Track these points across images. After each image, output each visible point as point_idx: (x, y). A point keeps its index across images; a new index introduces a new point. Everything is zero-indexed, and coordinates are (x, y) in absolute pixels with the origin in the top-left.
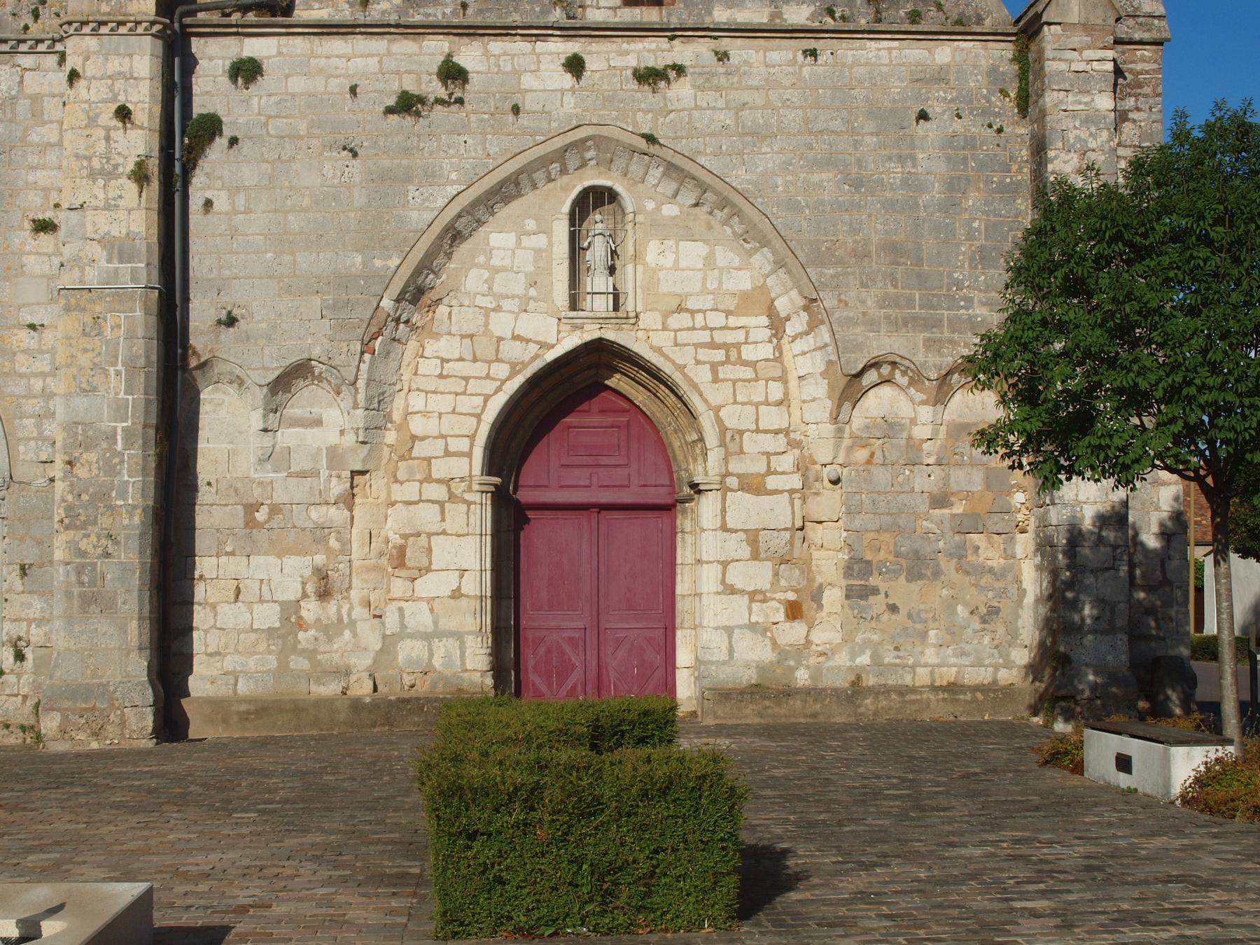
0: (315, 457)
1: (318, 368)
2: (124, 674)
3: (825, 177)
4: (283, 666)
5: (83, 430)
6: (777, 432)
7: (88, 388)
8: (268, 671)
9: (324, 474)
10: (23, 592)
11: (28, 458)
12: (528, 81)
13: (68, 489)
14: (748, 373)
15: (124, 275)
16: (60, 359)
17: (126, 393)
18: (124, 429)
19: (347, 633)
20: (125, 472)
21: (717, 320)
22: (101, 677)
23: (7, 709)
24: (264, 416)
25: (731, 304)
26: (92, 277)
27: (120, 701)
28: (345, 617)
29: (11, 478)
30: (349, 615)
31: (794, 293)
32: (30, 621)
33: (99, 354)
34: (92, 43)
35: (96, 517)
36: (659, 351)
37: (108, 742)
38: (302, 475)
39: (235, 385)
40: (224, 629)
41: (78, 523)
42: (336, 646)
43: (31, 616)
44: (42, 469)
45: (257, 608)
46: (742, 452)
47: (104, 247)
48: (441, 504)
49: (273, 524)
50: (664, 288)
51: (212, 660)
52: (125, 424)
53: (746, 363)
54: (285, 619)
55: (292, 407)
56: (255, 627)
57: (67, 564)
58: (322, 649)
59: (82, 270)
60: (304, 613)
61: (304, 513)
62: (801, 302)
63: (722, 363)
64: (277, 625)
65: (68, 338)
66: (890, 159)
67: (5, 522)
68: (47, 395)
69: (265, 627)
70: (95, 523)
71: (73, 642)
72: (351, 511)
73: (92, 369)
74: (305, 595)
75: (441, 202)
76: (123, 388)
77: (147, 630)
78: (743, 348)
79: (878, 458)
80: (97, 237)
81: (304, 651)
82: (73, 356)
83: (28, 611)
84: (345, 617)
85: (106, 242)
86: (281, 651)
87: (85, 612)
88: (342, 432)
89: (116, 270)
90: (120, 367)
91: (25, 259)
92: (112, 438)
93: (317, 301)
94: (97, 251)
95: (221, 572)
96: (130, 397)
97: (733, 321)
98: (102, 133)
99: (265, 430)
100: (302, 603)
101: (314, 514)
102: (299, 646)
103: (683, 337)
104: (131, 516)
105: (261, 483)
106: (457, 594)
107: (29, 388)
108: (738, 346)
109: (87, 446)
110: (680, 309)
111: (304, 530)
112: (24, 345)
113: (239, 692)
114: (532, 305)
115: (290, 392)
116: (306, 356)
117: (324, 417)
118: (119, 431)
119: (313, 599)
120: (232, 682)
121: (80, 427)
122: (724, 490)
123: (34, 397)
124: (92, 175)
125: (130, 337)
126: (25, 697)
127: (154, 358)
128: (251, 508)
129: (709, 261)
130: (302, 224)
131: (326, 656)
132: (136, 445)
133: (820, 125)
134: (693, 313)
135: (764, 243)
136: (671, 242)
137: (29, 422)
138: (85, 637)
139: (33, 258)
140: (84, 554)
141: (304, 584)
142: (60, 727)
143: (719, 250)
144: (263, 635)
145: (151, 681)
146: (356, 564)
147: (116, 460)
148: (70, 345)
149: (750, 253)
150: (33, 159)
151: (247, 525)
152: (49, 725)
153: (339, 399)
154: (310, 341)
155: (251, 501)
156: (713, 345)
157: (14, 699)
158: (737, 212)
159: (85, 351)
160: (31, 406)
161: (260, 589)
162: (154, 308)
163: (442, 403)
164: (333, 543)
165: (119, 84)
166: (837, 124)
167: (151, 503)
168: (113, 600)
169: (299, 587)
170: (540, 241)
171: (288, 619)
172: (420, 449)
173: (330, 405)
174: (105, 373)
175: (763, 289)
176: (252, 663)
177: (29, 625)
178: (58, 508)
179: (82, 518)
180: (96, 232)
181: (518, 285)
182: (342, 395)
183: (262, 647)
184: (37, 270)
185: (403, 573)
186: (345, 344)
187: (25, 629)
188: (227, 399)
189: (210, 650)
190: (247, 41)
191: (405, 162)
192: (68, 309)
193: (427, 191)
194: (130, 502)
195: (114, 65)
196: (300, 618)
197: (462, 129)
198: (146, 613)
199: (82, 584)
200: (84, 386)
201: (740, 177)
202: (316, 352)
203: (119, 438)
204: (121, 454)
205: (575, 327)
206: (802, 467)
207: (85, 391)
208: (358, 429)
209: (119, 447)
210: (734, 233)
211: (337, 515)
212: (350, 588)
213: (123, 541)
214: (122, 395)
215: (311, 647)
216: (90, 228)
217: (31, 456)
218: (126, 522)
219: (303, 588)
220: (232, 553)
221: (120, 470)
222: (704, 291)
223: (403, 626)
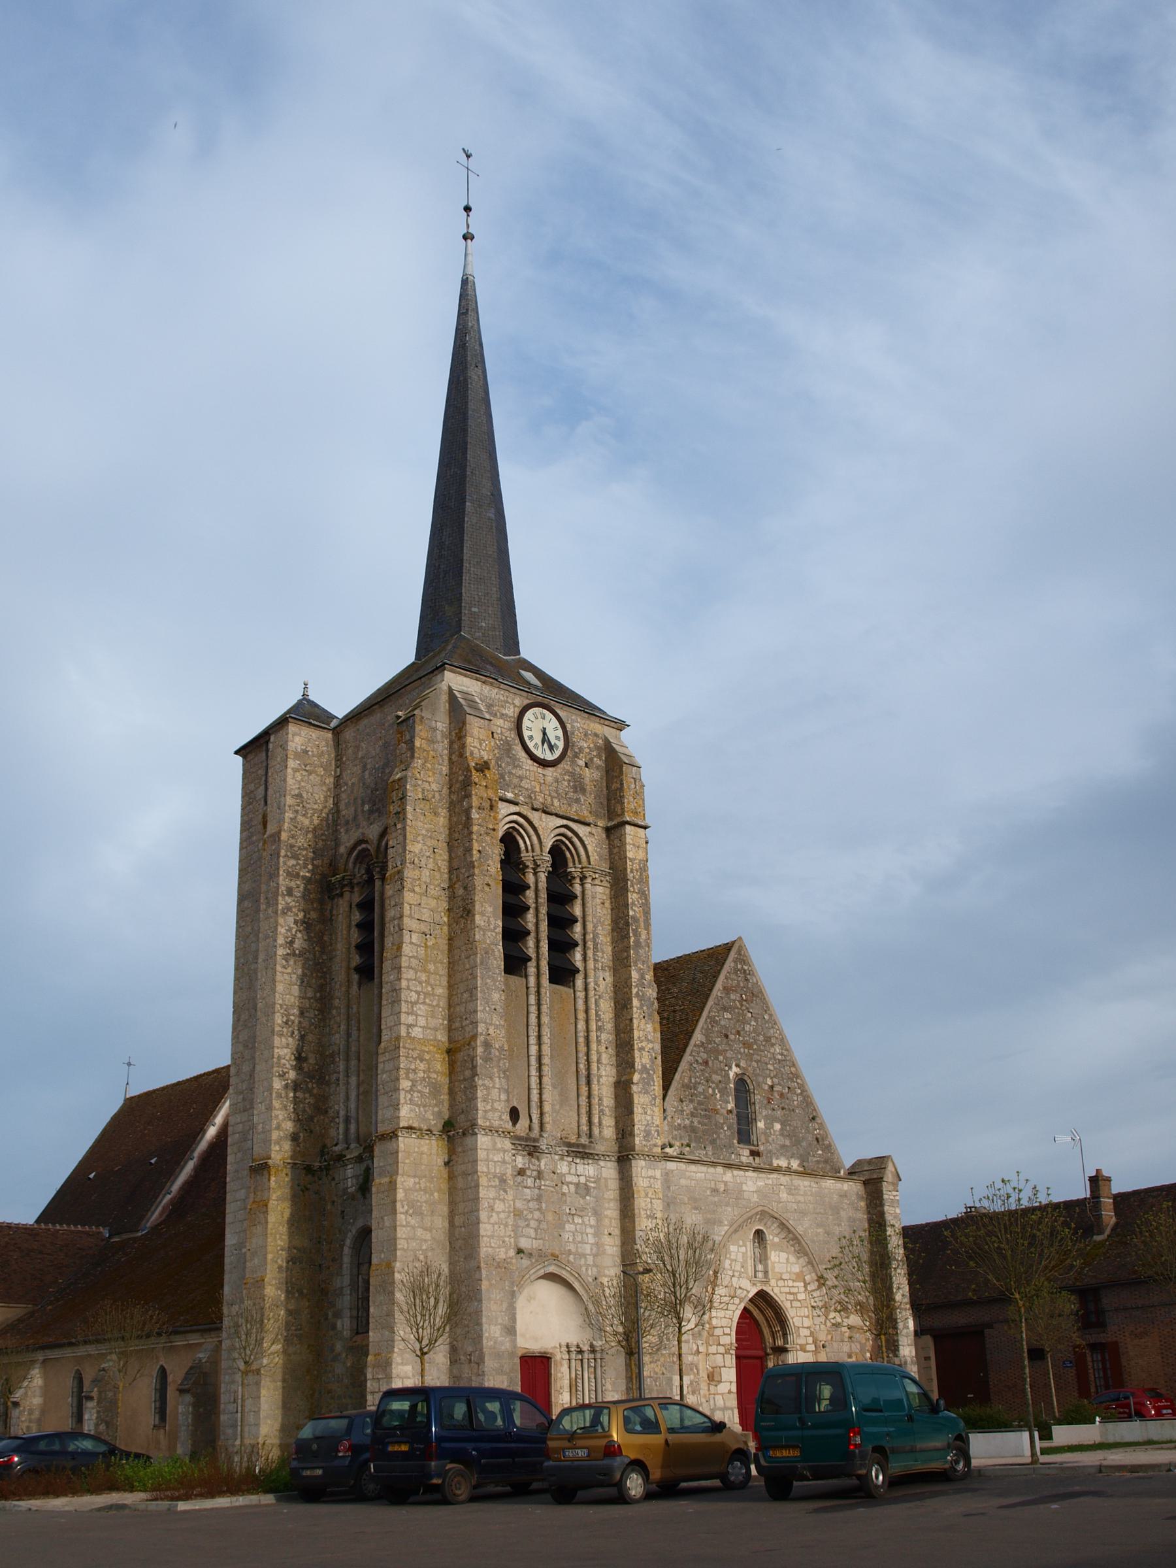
3: (820, 1230)
6: (807, 1328)
9: (691, 1341)
12: (745, 1187)
14: (799, 1304)
21: (791, 1283)
25: (794, 1277)
31: (814, 1275)
34: (642, 1163)
36: (776, 1294)
46: (799, 1336)
48: (723, 1354)
50: (777, 1270)
53: (799, 1301)
62: (816, 1278)
63: (793, 1300)
66: (835, 1225)
70: (659, 1360)
75: (723, 1233)
78: (798, 1295)
79: (834, 1339)
97: (796, 1284)
98: (649, 1200)
103: (783, 1290)
106: (730, 1392)
108: (796, 1293)
110: (781, 1279)
114: (743, 1275)
122: (796, 1351)
124: (648, 1217)
129: (788, 1259)
133: (818, 1211)
134: (784, 1280)
135: (806, 1254)
136: (777, 1253)
139: (608, 1247)
140: (657, 1374)
143: (790, 1256)
149: (798, 1258)
150: (607, 1205)
156: (790, 1293)
158: (799, 1243)
163: (721, 1314)
165: (652, 1180)
166: (822, 1211)
170: (743, 1249)
172: (718, 1332)
175: (802, 1272)
181: (738, 1268)
185: (714, 1383)
190: (668, 1163)
191: (713, 1216)
193: (720, 1228)
195: (651, 1172)
197: (727, 1205)
201: (800, 1229)
205: (754, 1284)
206: (815, 1342)
210: (795, 1250)
222: (787, 1272)
223: (715, 1405)
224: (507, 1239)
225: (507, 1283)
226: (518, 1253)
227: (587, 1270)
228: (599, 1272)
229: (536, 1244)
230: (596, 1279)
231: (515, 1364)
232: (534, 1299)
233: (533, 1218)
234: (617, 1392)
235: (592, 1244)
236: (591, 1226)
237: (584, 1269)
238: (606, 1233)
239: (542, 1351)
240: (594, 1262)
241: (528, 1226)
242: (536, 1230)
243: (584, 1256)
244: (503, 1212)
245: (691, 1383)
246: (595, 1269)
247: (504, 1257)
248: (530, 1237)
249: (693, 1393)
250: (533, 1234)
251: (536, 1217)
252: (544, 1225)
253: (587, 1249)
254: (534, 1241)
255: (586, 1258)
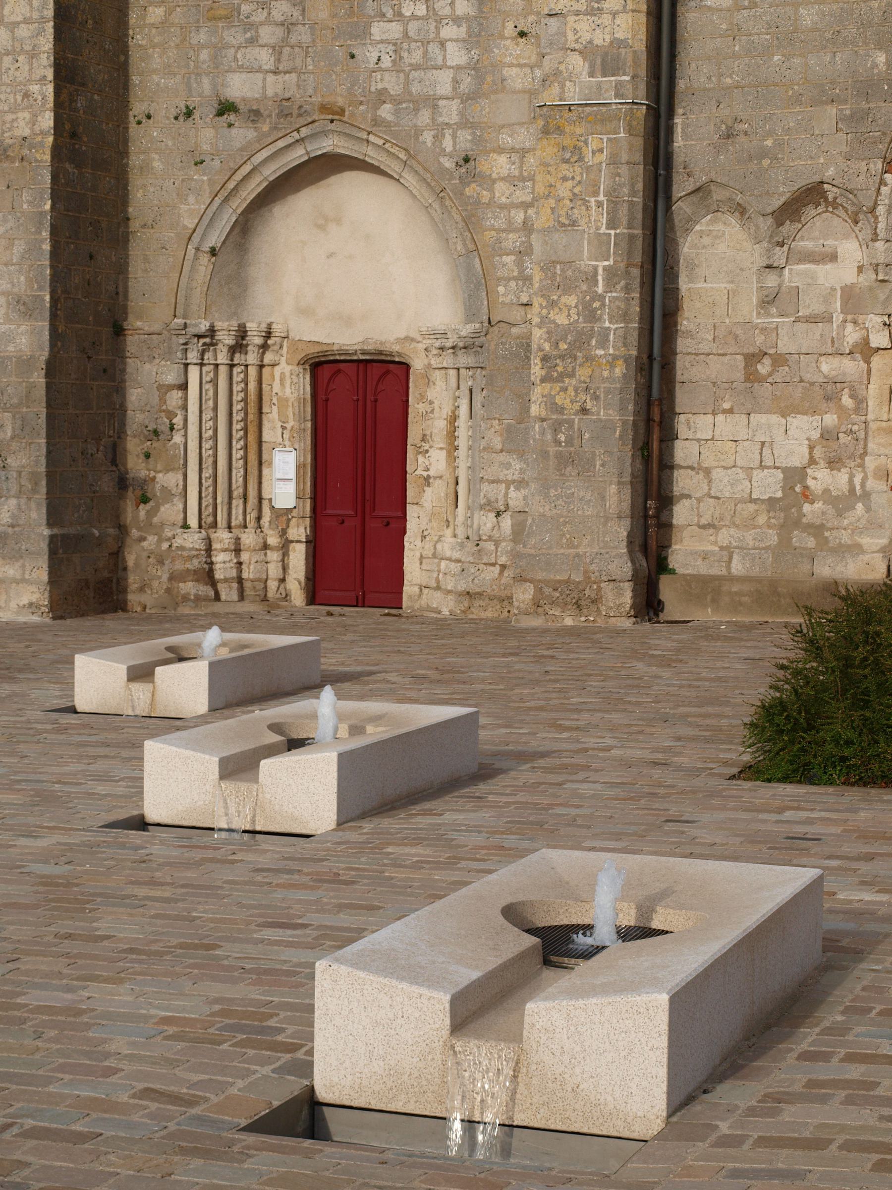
0: (827, 299)
1: (832, 193)
2: (602, 545)
4: (785, 541)
5: (562, 270)
7: (567, 222)
8: (766, 548)
9: (838, 318)
10: (502, 451)
11: (507, 300)
13: (545, 336)
15: (607, 90)
16: (540, 189)
17: (607, 228)
18: (605, 269)
19: (860, 506)
20: (606, 317)
22: (577, 547)
23: (484, 579)
24: (768, 250)
26: (573, 96)
27: (597, 574)
28: (858, 487)
29: (490, 323)
30: (863, 485)
32: (508, 484)
33: (580, 182)
35: (574, 368)
37: (583, 619)
38: (812, 319)
39: (737, 214)
40: (718, 498)
41: (555, 374)
42: (846, 522)
43: (510, 478)
44: (523, 313)
45: (757, 475)
47: (585, 59)
49: (777, 377)
51: (705, 532)
52: (606, 263)
54: (788, 488)
55: (802, 238)
56: (754, 496)
57: (543, 420)
58: (829, 525)
59: (563, 86)
60: (810, 482)
61: (814, 365)
64: (779, 494)
65: (547, 165)
67: (484, 373)
68: (527, 227)
69: (766, 497)
70: (572, 375)
71: (547, 508)
72: (868, 363)
73: (571, 200)
74: (812, 461)
76: (605, 222)
77: (628, 497)
80: (577, 46)
81: (810, 526)
82: (551, 186)
83: (506, 472)
84: (858, 487)
85: (587, 51)
86: (782, 526)
87: (562, 475)
88: (860, 269)
89: (599, 85)
90: (601, 198)
91: (506, 72)
92: (592, 279)
93: (832, 111)
94: (577, 62)
95: (717, 432)
96: (612, 232)
99: (769, 267)
100: (809, 471)
101: (827, 366)
102: (804, 520)
104: (612, 365)
105: (764, 330)
107: (510, 222)
109: (567, 287)
111: (812, 384)
112: (504, 172)
113: (733, 570)
115: (799, 221)
116: (817, 178)
117: (839, 250)
118: (600, 271)
119: (822, 465)
120: (726, 559)
121: (558, 267)
123: (515, 230)
125: (614, 161)
126: (503, 567)
127: (640, 186)
128: (752, 359)
130: (816, 18)
131: (835, 533)
132: (618, 287)
137: (509, 259)
138: (560, 502)
139: (515, 71)
140: (561, 410)
141: (811, 448)
142: (533, 599)
144: (763, 507)
145: (631, 552)
146: (873, 426)
147: (596, 304)
148: (549, 172)
151: (747, 379)
152: (521, 597)
153: (856, 229)
154: (822, 161)
155: (752, 350)
157: (492, 568)
159: (565, 179)
160: (513, 240)
161: (761, 454)
162: (640, 129)
164: (847, 401)
167: (634, 353)
168: (591, 462)
169: (806, 450)
171: (792, 488)
173: (846, 237)
174: (585, 202)
176: (749, 538)
177: (508, 488)
178: (535, 358)
179: (560, 369)
180: (577, 41)
182: (859, 224)
183: (762, 520)
184: (518, 85)
186: (864, 163)
187: (503, 491)
188: (727, 230)
189: (703, 521)
192: (546, 131)
194: (611, 351)
196: (806, 487)
198: (627, 478)
199: (558, 443)
200: (563, 220)
202: (831, 172)
203: (600, 278)
204: (601, 298)
207: (564, 225)
208: (877, 265)
209: (600, 289)
211: (851, 367)
212: (865, 453)
213: (602, 396)
214: (603, 230)
215: (818, 522)
216: (571, 36)
217: (511, 298)
218: (606, 374)
219: (810, 453)
220: (730, 411)
221: (601, 315)
224: (35, 88)
225: (26, 196)
226: (220, 113)
227: (438, 138)
228: (478, 141)
229: (274, 86)
230: (467, 160)
231: (31, 387)
232: (338, 221)
233: (269, 21)
234: (521, 455)
235: (458, 68)
236: (457, 20)
237: (428, 137)
238: (510, 30)
239: (370, 347)
240: (461, 114)
241: (253, 41)
242: (277, 51)
243: (432, 102)
244: (27, 21)
245: (827, 435)
246: (465, 136)
247: (27, 132)
248: (259, 70)
249: (834, 463)
250: (265, 58)
251: (277, 16)
252: (302, 35)
253: (443, 83)
254: (271, 78)
255: (435, 107)
